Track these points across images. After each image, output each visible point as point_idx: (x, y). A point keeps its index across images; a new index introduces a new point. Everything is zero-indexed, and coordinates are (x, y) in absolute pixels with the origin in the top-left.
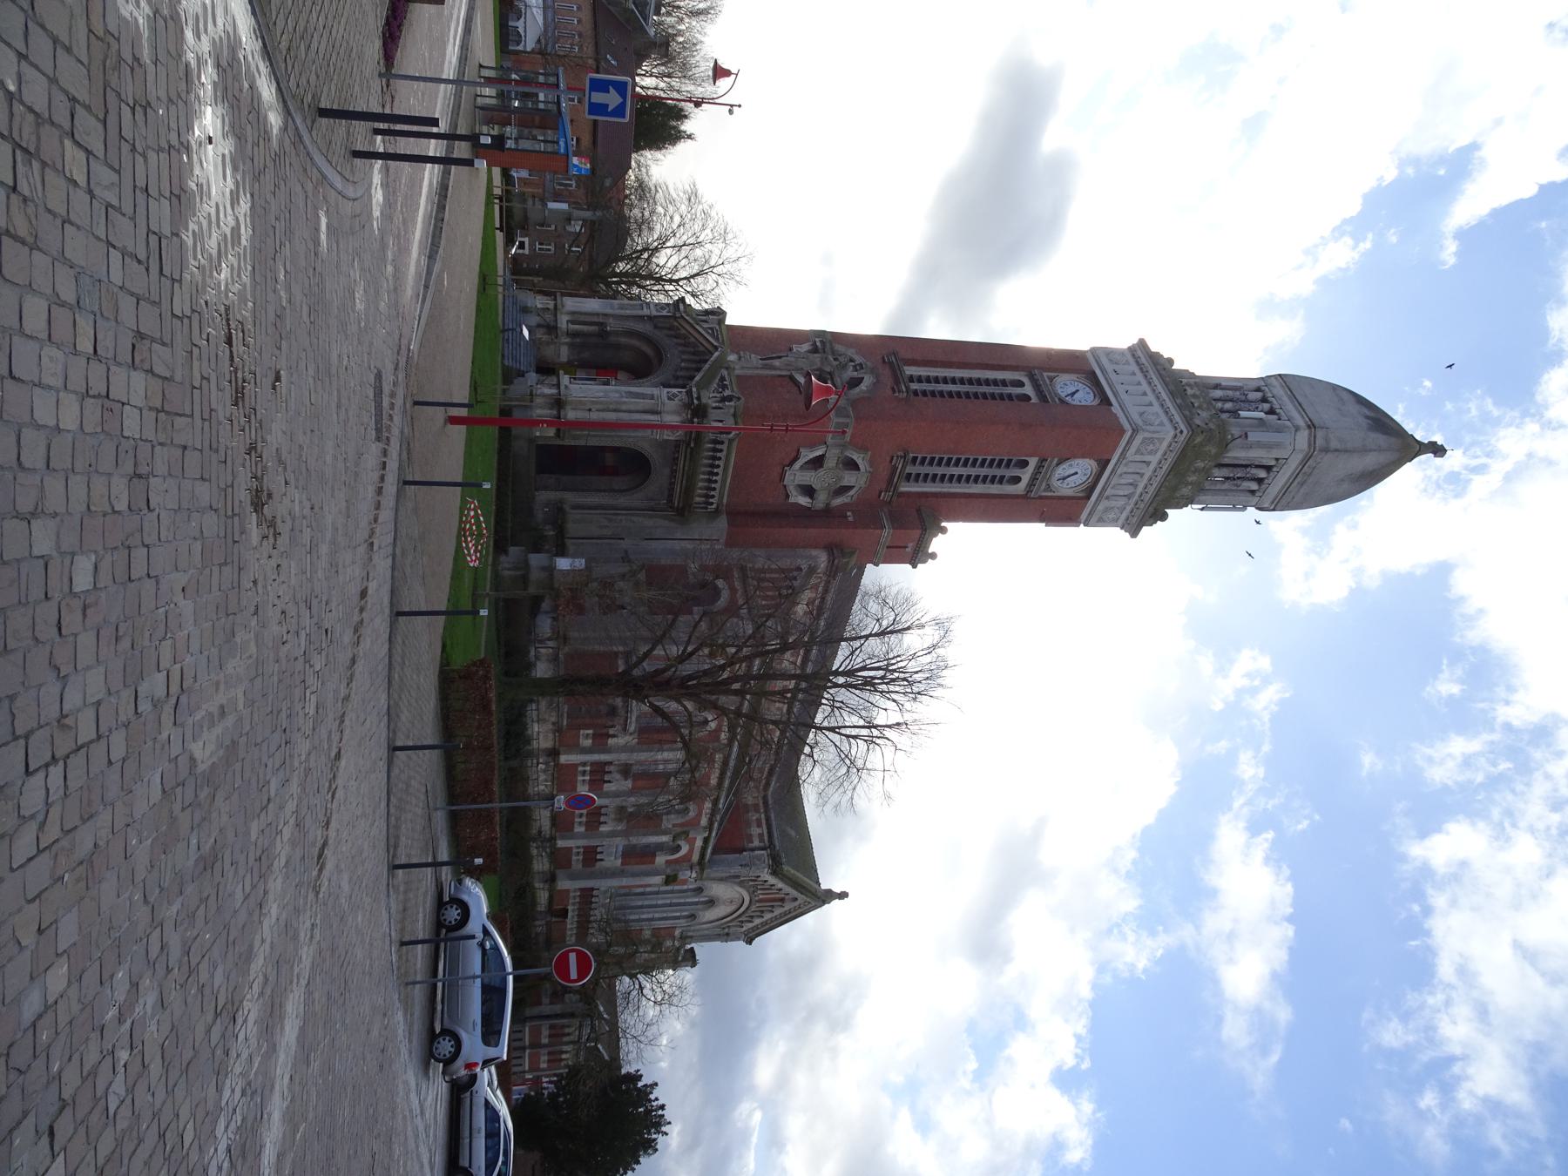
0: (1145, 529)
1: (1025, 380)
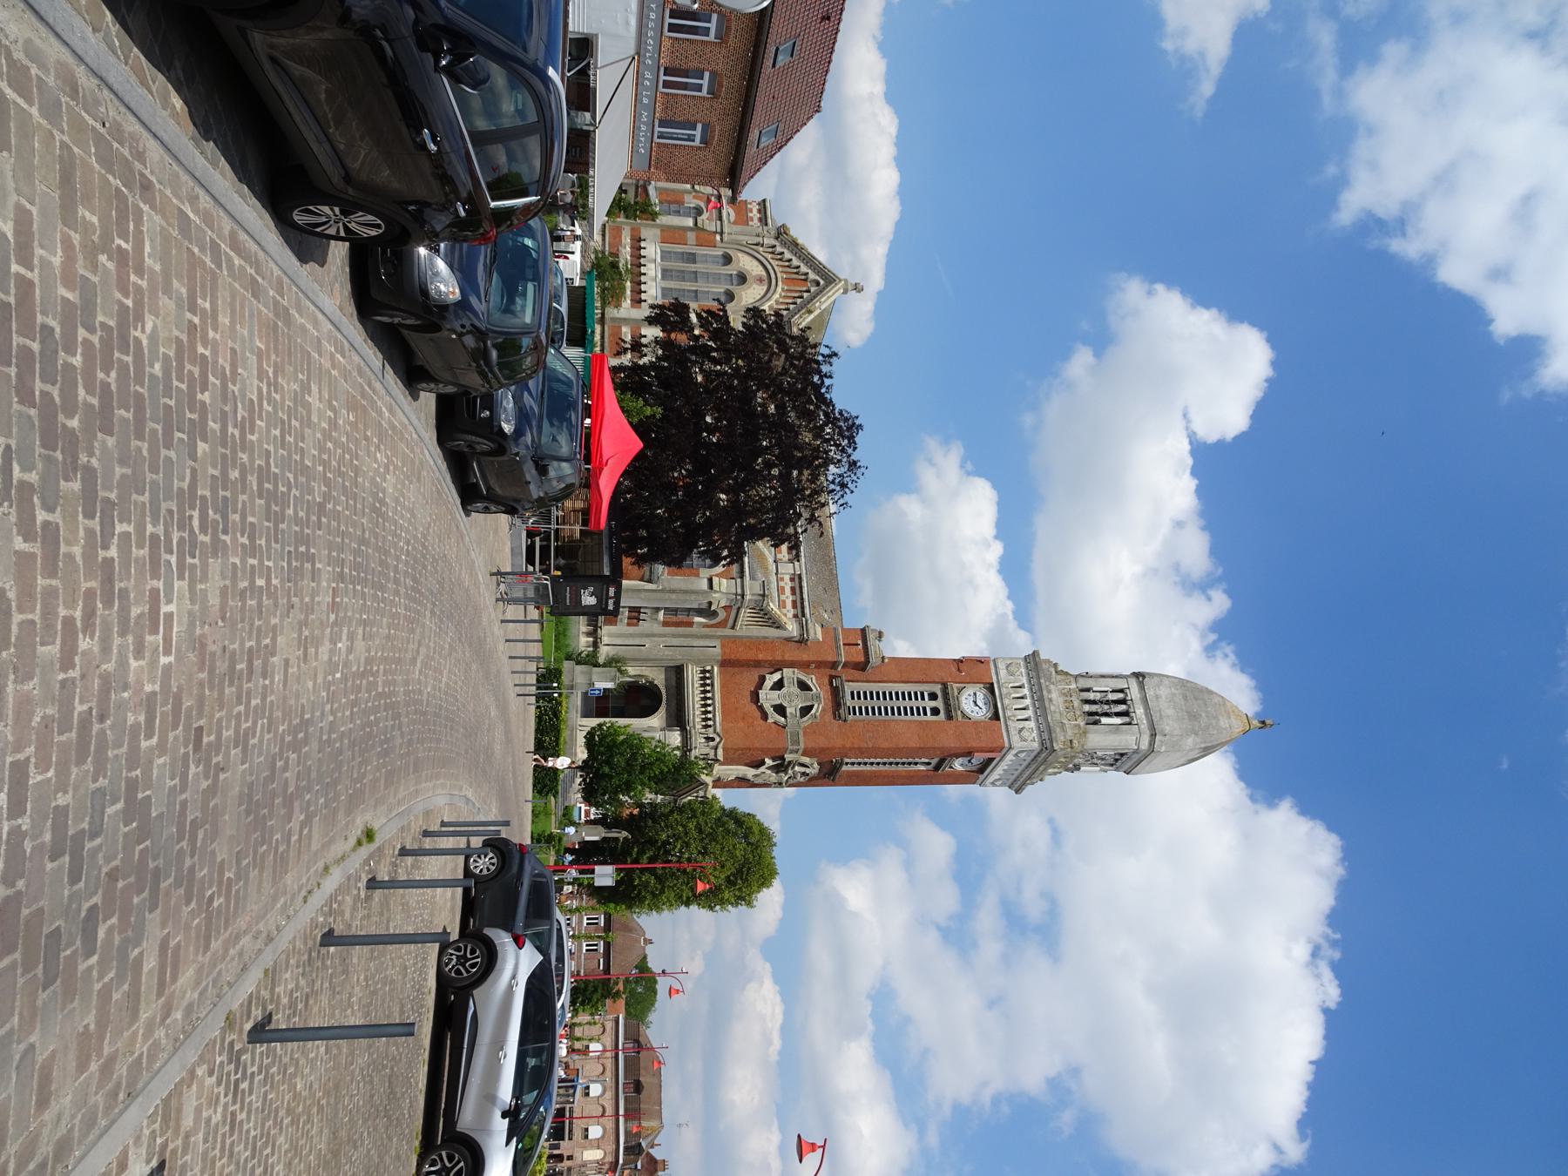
0: (1029, 788)
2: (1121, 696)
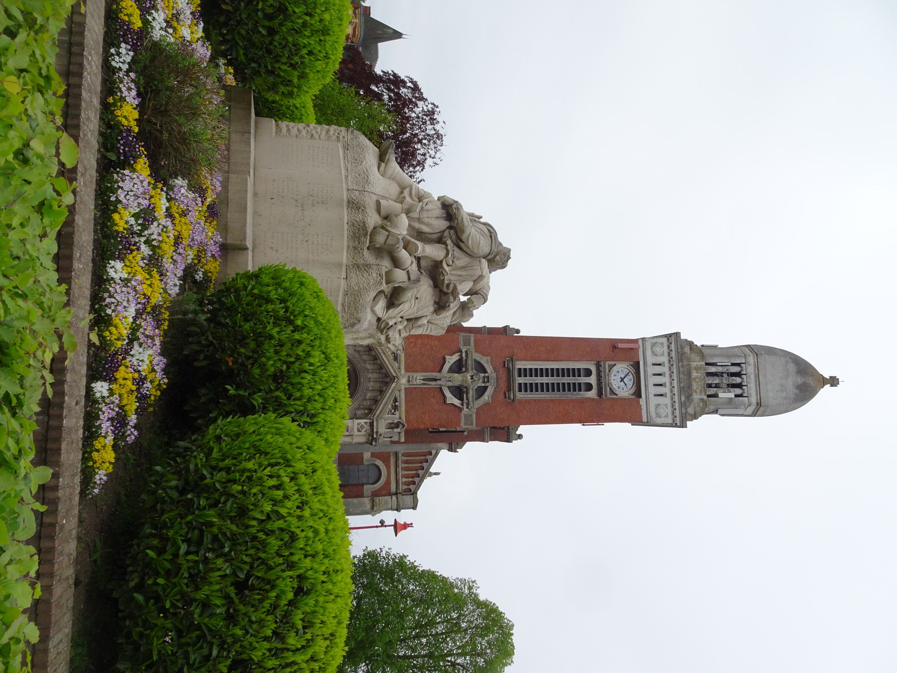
1: (593, 369)
2: (736, 369)
